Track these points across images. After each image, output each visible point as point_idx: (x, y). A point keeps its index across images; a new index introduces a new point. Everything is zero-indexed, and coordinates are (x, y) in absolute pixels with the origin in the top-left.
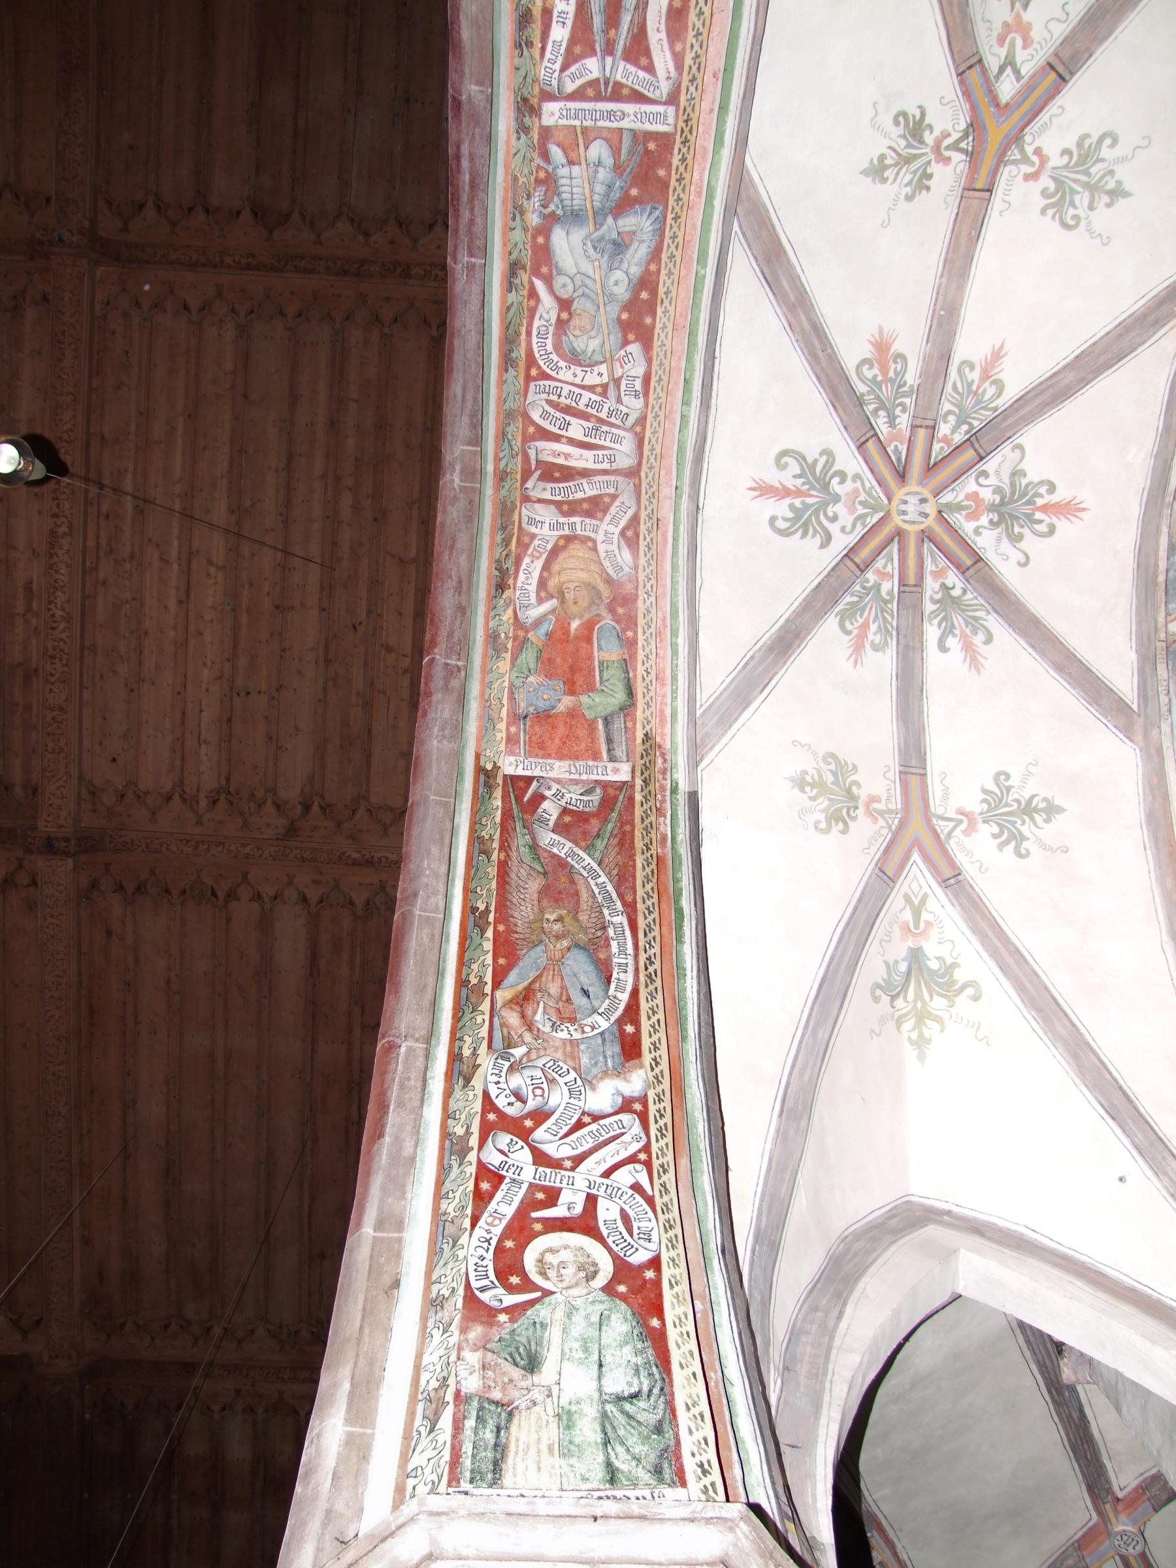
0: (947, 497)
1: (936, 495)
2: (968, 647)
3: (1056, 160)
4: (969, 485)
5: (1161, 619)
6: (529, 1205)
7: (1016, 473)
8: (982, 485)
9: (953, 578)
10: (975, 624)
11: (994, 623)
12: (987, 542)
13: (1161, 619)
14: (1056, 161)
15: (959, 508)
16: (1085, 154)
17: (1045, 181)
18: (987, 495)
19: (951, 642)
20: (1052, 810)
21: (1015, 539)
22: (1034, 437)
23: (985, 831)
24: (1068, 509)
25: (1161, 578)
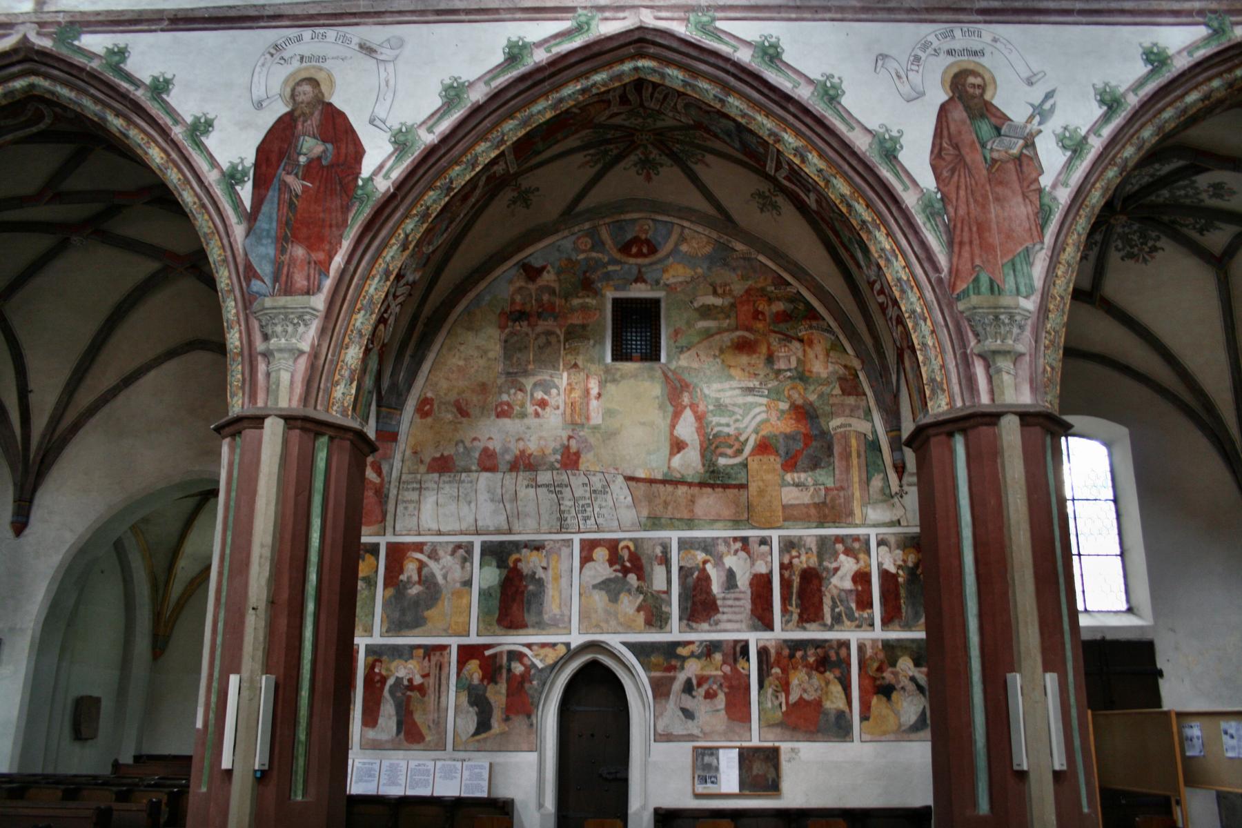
0: (650, 147)
1: (652, 144)
2: (588, 162)
3: (774, 199)
4: (655, 152)
5: (607, 220)
6: (386, 311)
7: (662, 165)
8: (654, 154)
9: (615, 152)
10: (596, 163)
11: (599, 166)
12: (633, 158)
13: (607, 220)
14: (774, 199)
15: (645, 147)
16: (775, 206)
17: (767, 194)
18: (652, 156)
19: (589, 158)
20: (528, 207)
21: (635, 165)
22: (676, 170)
23: (515, 194)
24: (649, 178)
25: (623, 217)
